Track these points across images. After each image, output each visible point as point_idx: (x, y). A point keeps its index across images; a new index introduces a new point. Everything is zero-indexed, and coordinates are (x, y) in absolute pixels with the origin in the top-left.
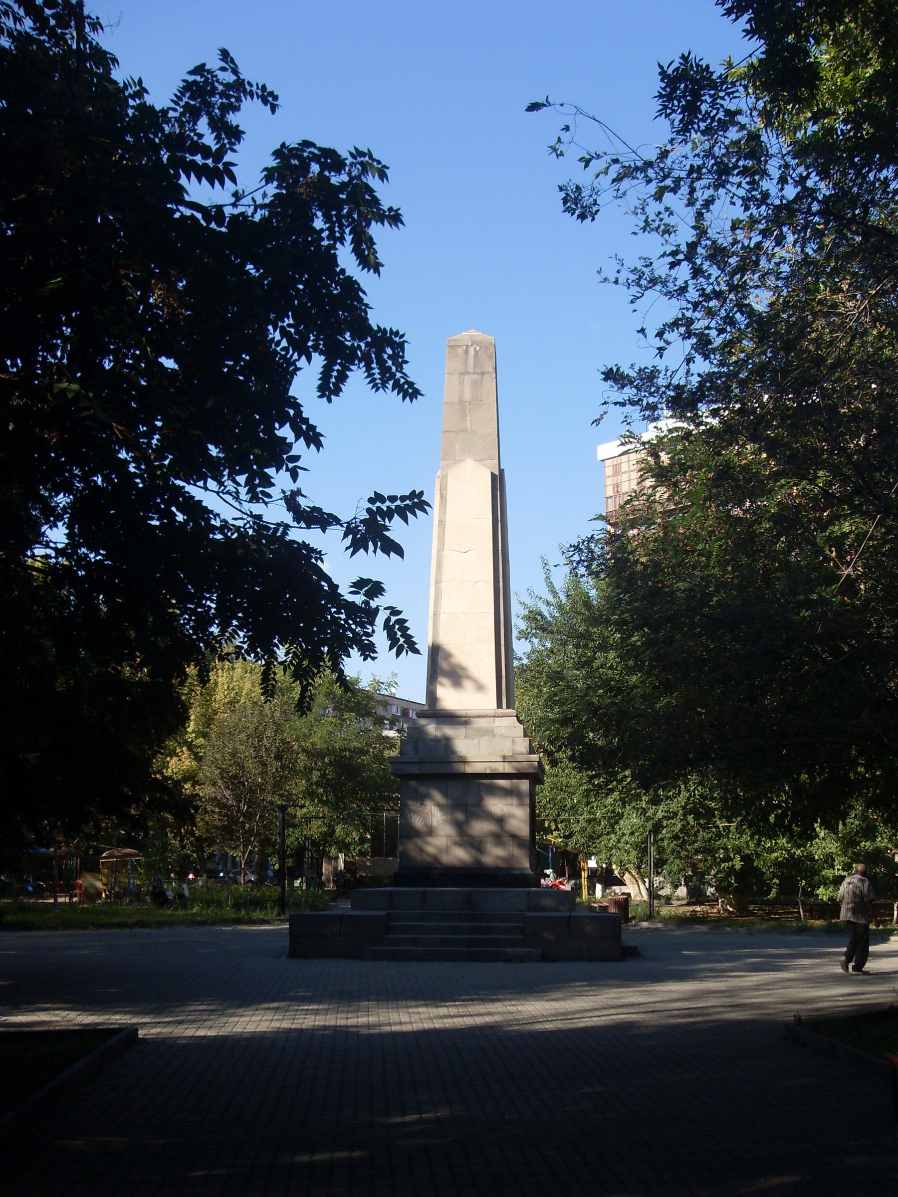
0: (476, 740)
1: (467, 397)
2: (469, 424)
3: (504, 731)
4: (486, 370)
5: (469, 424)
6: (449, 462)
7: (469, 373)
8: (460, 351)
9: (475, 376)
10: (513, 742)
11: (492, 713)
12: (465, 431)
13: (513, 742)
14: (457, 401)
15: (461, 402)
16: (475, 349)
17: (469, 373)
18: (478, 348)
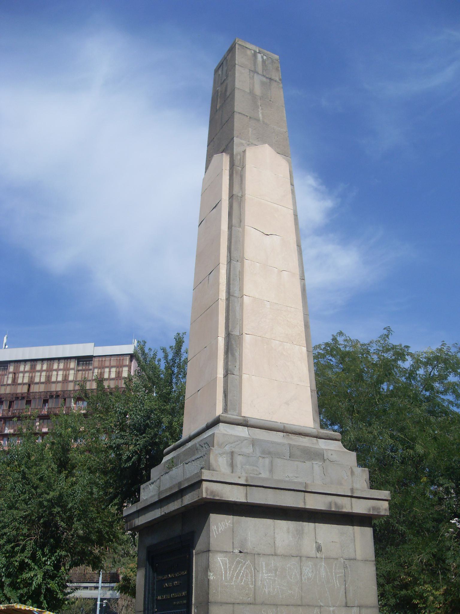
0: (308, 464)
1: (258, 90)
2: (260, 115)
3: (334, 457)
4: (273, 78)
5: (260, 115)
6: (243, 142)
7: (258, 73)
8: (249, 52)
9: (264, 79)
10: (352, 473)
11: (314, 432)
12: (258, 120)
13: (352, 473)
14: (247, 90)
15: (252, 93)
16: (262, 57)
17: (258, 73)
18: (265, 58)
